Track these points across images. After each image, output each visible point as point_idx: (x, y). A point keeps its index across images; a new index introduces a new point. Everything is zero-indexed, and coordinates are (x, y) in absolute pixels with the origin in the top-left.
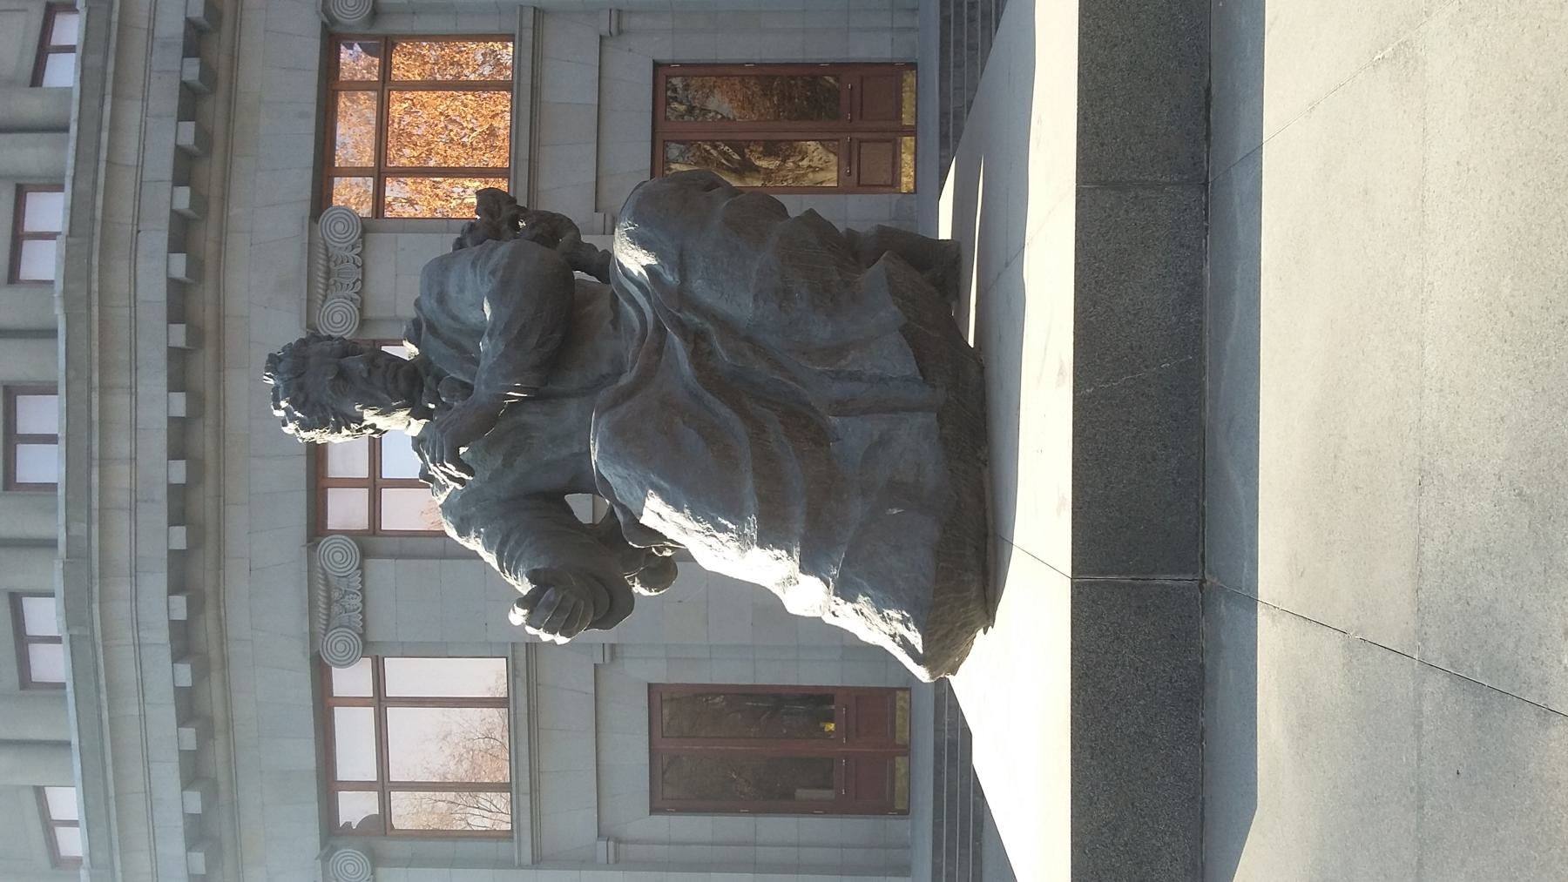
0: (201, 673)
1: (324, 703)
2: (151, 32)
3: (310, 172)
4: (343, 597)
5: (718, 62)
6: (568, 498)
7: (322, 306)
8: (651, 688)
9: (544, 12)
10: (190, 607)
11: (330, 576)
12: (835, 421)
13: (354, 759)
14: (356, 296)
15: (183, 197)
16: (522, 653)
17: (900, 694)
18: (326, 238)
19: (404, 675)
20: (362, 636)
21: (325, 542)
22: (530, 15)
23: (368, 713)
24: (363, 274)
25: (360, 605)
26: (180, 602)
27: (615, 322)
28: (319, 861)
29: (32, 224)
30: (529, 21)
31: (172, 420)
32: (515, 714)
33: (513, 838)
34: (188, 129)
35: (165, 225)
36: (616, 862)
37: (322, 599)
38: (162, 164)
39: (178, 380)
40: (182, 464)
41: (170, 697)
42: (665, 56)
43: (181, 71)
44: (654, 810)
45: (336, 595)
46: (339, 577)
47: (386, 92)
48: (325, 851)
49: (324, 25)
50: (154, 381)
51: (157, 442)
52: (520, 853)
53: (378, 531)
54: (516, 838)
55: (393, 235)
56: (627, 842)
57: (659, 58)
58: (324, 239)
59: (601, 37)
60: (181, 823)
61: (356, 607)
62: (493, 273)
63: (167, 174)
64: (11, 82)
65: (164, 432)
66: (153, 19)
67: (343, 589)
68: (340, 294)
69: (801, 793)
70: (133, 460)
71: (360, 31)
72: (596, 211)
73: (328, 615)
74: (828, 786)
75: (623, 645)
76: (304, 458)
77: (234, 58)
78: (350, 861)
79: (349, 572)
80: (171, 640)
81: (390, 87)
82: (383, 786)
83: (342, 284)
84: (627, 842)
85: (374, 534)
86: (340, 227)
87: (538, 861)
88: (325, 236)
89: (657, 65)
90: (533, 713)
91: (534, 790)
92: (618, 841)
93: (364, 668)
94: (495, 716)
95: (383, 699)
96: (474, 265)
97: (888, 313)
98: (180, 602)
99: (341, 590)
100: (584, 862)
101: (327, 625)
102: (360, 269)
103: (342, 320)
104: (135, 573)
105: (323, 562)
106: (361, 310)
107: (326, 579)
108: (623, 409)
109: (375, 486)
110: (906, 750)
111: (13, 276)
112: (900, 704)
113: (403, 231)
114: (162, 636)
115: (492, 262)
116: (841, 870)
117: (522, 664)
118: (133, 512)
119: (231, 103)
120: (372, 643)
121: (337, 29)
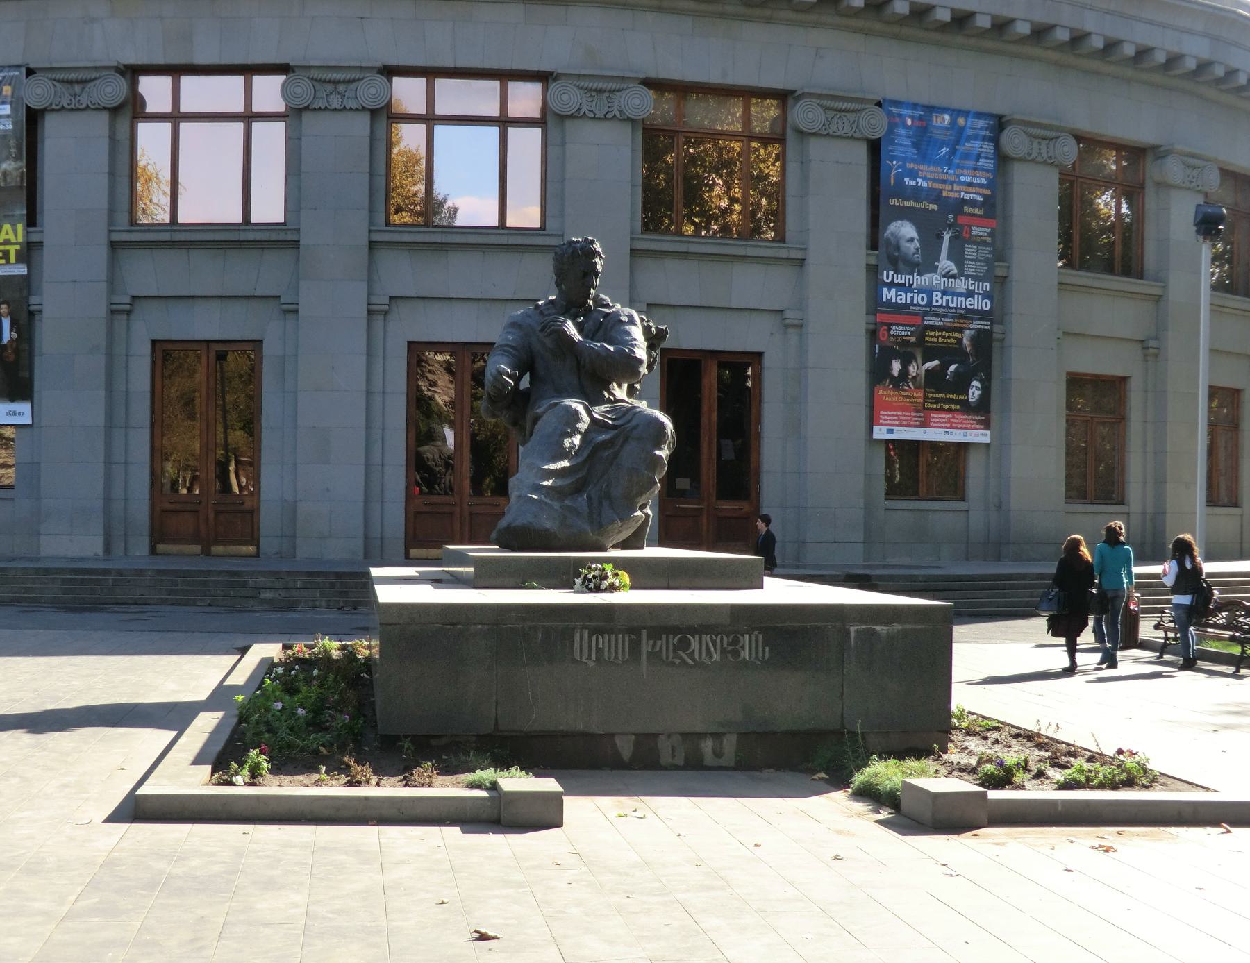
1: (248, 70)
3: (680, 78)
4: (339, 94)
5: (762, 404)
7: (574, 85)
9: (802, 266)
11: (357, 83)
12: (585, 496)
14: (582, 112)
16: (290, 237)
18: (627, 91)
20: (307, 108)
21: (382, 79)
22: (799, 255)
23: (239, 108)
24: (600, 119)
25: (333, 107)
28: (115, 64)
32: (239, 230)
33: (132, 225)
36: (113, 312)
37: (344, 76)
44: (154, 342)
45: (341, 88)
46: (356, 90)
47: (742, 138)
48: (122, 67)
49: (793, 92)
52: (120, 231)
53: (391, 120)
54: (133, 228)
55: (630, 142)
56: (128, 320)
57: (766, 356)
58: (626, 89)
59: (782, 311)
61: (330, 103)
67: (346, 94)
71: (789, 119)
72: (648, 305)
73: (325, 81)
75: (297, 320)
78: (115, 90)
79: (359, 99)
81: (745, 142)
82: (176, 117)
83: (592, 101)
84: (128, 320)
85: (388, 118)
87: (114, 246)
88: (630, 90)
90: (239, 244)
92: (129, 312)
94: (237, 218)
95: (250, 120)
99: (345, 92)
101: (316, 80)
102: (603, 117)
103: (563, 101)
105: (369, 78)
106: (571, 116)
107: (354, 81)
109: (429, 119)
116: (108, 499)
117: (282, 237)
119: (734, 17)
121: (790, 101)
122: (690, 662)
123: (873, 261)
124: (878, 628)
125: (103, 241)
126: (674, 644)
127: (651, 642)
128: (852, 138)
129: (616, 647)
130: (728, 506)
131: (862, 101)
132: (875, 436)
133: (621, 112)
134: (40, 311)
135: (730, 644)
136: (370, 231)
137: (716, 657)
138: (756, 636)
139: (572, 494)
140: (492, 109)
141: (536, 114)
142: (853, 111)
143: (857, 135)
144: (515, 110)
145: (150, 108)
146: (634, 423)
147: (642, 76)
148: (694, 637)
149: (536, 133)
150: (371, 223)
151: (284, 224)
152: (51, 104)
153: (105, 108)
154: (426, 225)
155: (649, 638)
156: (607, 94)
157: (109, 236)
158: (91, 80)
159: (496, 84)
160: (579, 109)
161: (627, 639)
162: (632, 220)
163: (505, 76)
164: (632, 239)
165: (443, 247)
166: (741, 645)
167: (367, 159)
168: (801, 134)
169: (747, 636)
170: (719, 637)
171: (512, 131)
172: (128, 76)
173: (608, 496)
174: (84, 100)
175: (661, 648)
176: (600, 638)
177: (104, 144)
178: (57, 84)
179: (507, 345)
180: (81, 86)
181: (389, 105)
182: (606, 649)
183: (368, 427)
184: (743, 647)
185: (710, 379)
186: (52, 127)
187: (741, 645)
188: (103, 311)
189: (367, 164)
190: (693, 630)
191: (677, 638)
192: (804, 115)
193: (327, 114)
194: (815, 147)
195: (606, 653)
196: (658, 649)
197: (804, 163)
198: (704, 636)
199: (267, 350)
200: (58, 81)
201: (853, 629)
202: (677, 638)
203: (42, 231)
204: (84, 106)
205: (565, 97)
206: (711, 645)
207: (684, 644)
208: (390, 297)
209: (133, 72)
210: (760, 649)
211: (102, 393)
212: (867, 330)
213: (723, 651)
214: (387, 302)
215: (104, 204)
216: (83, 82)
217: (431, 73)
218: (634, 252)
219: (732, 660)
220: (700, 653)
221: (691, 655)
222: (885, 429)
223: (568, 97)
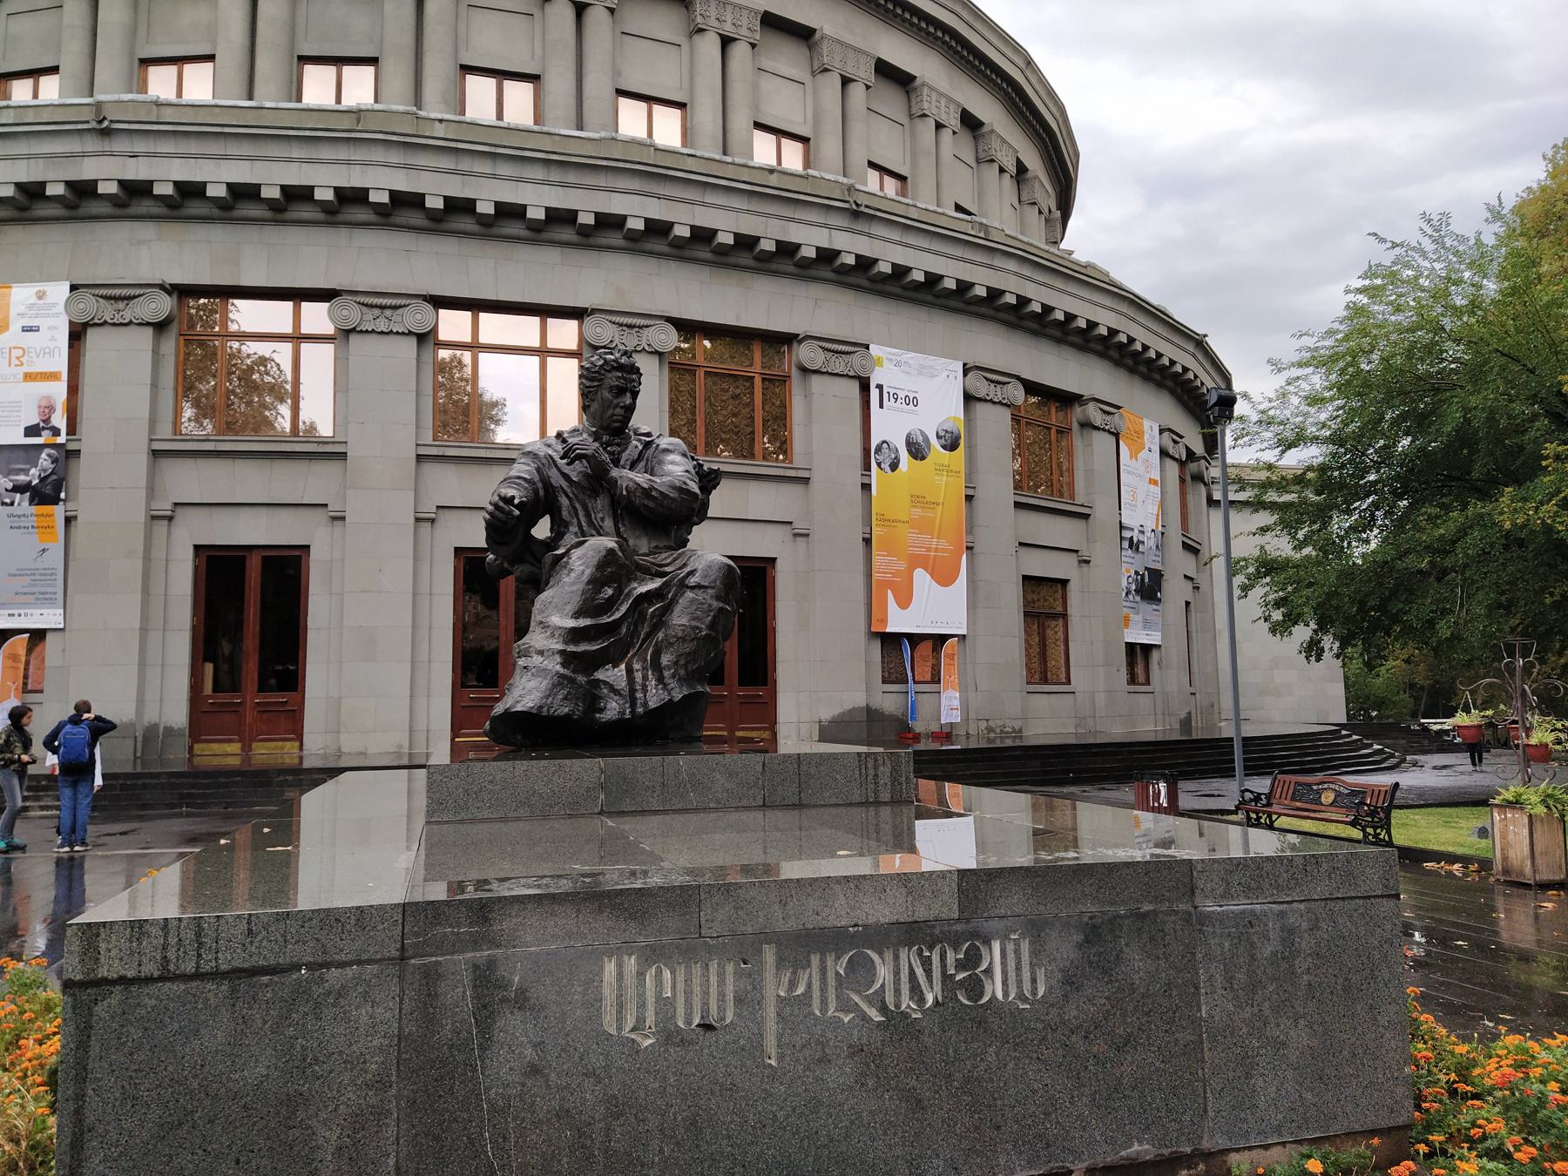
1: (297, 295)
2: (792, 220)
6: (547, 518)
20: (353, 330)
22: (805, 474)
25: (379, 330)
30: (800, 474)
36: (154, 518)
38: (705, 219)
40: (492, 211)
42: (779, 565)
44: (197, 548)
45: (388, 313)
48: (168, 286)
53: (437, 347)
57: (778, 560)
59: (791, 523)
62: (685, 483)
63: (698, 223)
64: (756, 107)
66: (800, 222)
69: (209, 668)
70: (494, 177)
74: (217, 688)
84: (169, 525)
87: (156, 454)
89: (774, 560)
92: (170, 519)
96: (687, 471)
97: (677, 696)
101: (363, 304)
108: (620, 554)
111: (621, 93)
112: (288, 745)
115: (688, 482)
120: (348, 340)
121: (795, 345)
125: (145, 449)
126: (837, 973)
127: (786, 978)
128: (847, 376)
129: (706, 994)
134: (75, 517)
135: (960, 966)
136: (417, 445)
138: (1017, 943)
141: (572, 345)
144: (552, 343)
148: (881, 954)
152: (93, 318)
153: (148, 324)
155: (781, 962)
156: (637, 329)
157: (150, 445)
158: (135, 297)
160: (612, 341)
161: (730, 968)
166: (984, 966)
167: (415, 379)
168: (804, 370)
169: (996, 946)
170: (938, 947)
171: (551, 360)
172: (175, 297)
174: (128, 317)
175: (809, 986)
176: (667, 974)
178: (100, 300)
179: (519, 478)
180: (126, 302)
181: (435, 330)
182: (681, 1000)
183: (414, 626)
184: (989, 971)
186: (93, 337)
187: (984, 966)
188: (141, 516)
191: (846, 958)
192: (806, 354)
193: (373, 336)
194: (816, 381)
195: (681, 1011)
196: (800, 990)
197: (808, 396)
198: (903, 954)
199: (314, 554)
200: (102, 297)
202: (846, 958)
203: (80, 440)
204: (126, 321)
206: (919, 972)
207: (861, 970)
210: (1026, 975)
211: (138, 597)
213: (946, 978)
214: (434, 510)
215: (146, 414)
217: (476, 306)
219: (965, 1002)
220: (897, 992)
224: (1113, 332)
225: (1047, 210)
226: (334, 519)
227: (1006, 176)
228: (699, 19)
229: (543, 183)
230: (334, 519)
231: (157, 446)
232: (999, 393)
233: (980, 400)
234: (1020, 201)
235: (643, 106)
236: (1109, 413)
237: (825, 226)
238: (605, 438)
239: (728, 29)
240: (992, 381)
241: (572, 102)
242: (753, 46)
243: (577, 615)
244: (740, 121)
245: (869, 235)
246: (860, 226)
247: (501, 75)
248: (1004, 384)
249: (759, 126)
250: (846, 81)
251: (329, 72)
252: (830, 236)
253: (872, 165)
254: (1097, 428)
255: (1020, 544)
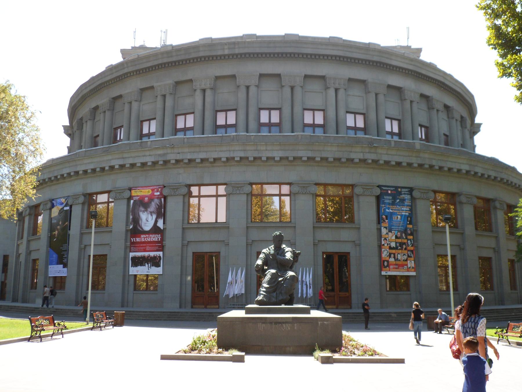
0: (224, 162)
1: (217, 185)
8: (219, 252)
10: (237, 161)
13: (206, 190)
15: (318, 159)
16: (227, 226)
17: (217, 306)
19: (222, 201)
22: (358, 226)
23: (215, 194)
26: (238, 159)
27: (285, 270)
29: (316, 113)
31: (274, 157)
34: (332, 160)
35: (313, 156)
38: (324, 155)
39: (281, 158)
40: (266, 159)
41: (219, 156)
42: (351, 255)
43: (343, 158)
44: (193, 253)
45: (239, 188)
49: (355, 184)
50: (281, 154)
51: (270, 155)
56: (187, 247)
59: (354, 241)
60: (194, 158)
65: (272, 156)
68: (300, 189)
70: (266, 150)
76: (267, 182)
77: (347, 167)
78: (184, 190)
80: (231, 157)
82: (199, 196)
84: (187, 247)
85: (251, 195)
86: (313, 189)
87: (183, 229)
89: (349, 253)
90: (214, 228)
91: (198, 228)
93: (224, 193)
98: (238, 159)
100: (183, 239)
104: (244, 150)
107: (242, 187)
110: (206, 308)
113: (313, 202)
114: (232, 155)
115: (291, 258)
116: (181, 293)
117: (225, 226)
118: (256, 150)
121: (354, 187)
122: (283, 330)
123: (379, 227)
124: (325, 322)
125: (181, 227)
130: (342, 294)
131: (373, 186)
132: (382, 274)
133: (309, 192)
134: (165, 245)
136: (247, 224)
137: (289, 329)
139: (272, 292)
140: (277, 192)
141: (288, 192)
142: (371, 189)
143: (372, 195)
144: (283, 192)
145: (193, 195)
146: (288, 276)
147: (314, 183)
149: (289, 197)
150: (247, 222)
151: (225, 222)
154: (261, 222)
155: (274, 324)
159: (278, 186)
160: (299, 192)
162: (313, 219)
163: (280, 184)
164: (313, 224)
165: (265, 227)
167: (246, 206)
173: (281, 293)
174: (177, 193)
177: (181, 204)
181: (251, 192)
184: (295, 326)
185: (336, 260)
186: (169, 200)
188: (180, 246)
189: (246, 207)
190: (284, 323)
192: (357, 190)
194: (361, 199)
197: (358, 202)
199: (222, 254)
200: (171, 189)
201: (319, 323)
205: (295, 189)
208: (252, 241)
209: (189, 186)
212: (378, 246)
214: (251, 241)
215: (181, 218)
216: (177, 189)
218: (314, 227)
221: (284, 328)
222: (385, 272)
223: (296, 189)
224: (468, 172)
225: (459, 119)
226: (226, 245)
227: (440, 112)
228: (328, 85)
229: (279, 150)
230: (226, 245)
231: (184, 227)
232: (425, 197)
233: (418, 198)
234: (448, 118)
235: (312, 112)
236: (469, 198)
237: (362, 152)
238: (277, 249)
239: (337, 86)
240: (422, 192)
241: (290, 115)
242: (345, 89)
243: (268, 284)
244: (342, 112)
245: (376, 153)
246: (373, 151)
247: (270, 109)
248: (426, 193)
249: (347, 112)
250: (376, 95)
251: (223, 114)
252: (363, 155)
253: (387, 118)
254: (465, 203)
255: (436, 244)
